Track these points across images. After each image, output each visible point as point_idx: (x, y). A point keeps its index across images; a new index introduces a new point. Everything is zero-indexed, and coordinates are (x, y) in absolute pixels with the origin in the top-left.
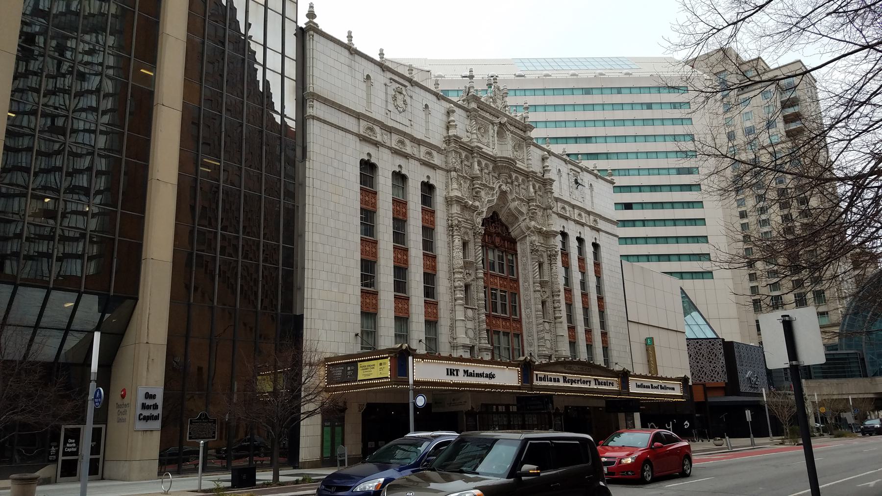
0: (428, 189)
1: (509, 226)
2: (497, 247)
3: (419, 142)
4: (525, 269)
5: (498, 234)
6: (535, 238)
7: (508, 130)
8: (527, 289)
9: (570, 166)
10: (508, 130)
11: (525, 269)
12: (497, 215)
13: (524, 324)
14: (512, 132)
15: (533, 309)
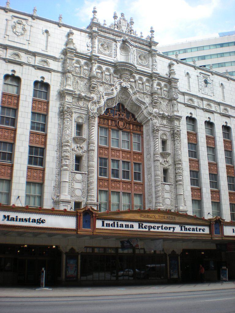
0: (42, 86)
1: (135, 114)
2: (121, 129)
3: (34, 54)
4: (148, 145)
5: (121, 119)
6: (157, 122)
7: (131, 45)
8: (149, 160)
9: (200, 71)
10: (131, 45)
11: (148, 145)
12: (123, 106)
13: (146, 186)
15: (153, 175)
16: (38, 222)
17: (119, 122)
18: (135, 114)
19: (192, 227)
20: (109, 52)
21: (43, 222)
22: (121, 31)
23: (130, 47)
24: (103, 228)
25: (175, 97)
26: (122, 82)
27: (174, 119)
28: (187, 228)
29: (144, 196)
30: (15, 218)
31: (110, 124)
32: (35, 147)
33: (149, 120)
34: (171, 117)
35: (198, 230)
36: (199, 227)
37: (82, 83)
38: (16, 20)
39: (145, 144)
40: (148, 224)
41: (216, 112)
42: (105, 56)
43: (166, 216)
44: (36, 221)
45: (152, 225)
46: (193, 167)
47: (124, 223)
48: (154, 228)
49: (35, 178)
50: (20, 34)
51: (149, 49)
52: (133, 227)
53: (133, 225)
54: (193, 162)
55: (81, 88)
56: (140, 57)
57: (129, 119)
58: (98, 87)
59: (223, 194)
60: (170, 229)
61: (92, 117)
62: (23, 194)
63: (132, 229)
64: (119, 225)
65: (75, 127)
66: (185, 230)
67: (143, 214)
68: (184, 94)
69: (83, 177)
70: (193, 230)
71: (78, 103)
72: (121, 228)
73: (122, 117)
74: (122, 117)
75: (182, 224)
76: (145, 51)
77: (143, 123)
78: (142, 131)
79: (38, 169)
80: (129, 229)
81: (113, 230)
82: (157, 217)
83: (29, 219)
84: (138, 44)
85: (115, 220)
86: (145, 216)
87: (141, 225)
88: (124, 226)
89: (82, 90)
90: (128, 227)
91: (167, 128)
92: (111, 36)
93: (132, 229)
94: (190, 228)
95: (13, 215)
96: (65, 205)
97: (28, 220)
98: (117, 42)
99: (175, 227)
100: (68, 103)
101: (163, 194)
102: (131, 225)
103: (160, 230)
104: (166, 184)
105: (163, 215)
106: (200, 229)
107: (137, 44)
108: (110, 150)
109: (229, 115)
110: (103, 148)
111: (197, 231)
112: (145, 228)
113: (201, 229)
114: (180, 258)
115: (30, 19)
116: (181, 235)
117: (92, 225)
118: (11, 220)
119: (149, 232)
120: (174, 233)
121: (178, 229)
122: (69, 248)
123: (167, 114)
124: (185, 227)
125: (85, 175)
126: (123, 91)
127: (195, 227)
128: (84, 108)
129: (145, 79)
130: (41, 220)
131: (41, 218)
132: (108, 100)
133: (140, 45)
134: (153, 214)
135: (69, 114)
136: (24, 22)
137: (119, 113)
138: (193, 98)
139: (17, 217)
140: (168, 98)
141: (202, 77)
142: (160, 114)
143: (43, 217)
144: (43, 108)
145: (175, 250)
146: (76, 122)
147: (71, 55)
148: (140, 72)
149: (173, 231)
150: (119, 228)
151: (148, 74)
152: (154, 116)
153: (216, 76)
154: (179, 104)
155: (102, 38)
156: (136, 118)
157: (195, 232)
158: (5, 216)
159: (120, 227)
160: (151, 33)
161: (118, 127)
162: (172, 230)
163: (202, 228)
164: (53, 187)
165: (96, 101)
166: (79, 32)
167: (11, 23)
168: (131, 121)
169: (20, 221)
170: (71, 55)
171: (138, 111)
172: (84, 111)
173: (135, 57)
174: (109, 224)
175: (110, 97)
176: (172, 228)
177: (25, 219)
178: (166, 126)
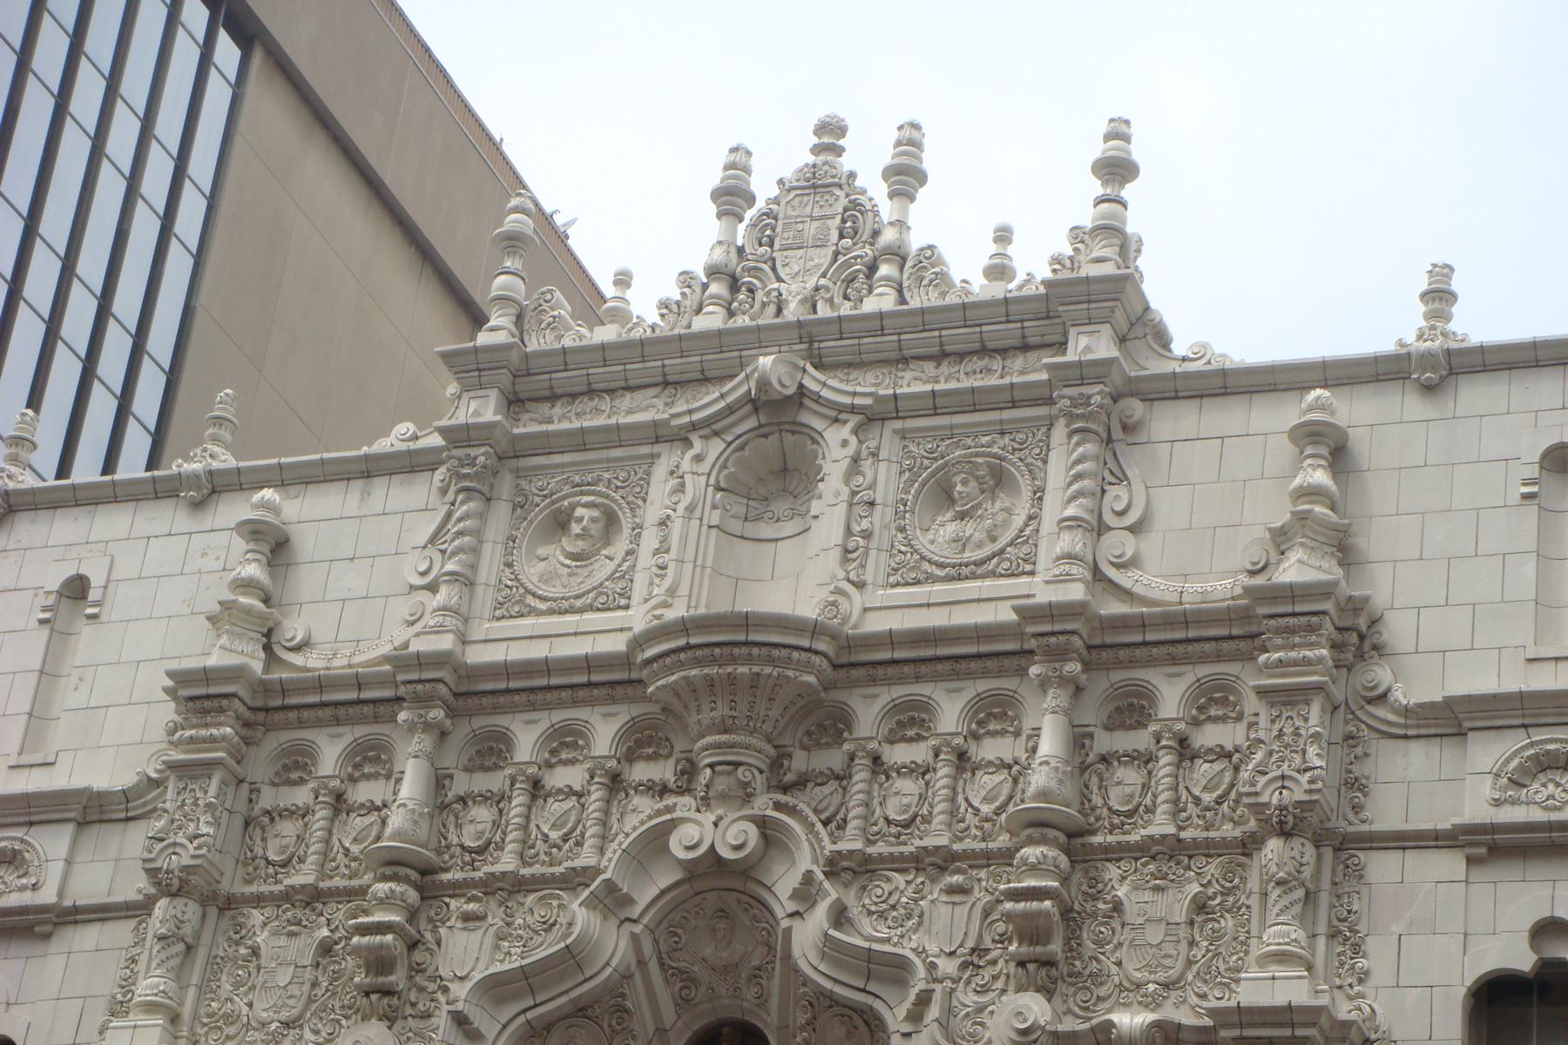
10: (838, 413)
14: (871, 417)
22: (768, 318)
25: (1264, 799)
26: (673, 824)
58: (439, 944)
76: (1008, 414)
84: (929, 367)
107: (912, 383)
147: (203, 732)
151: (983, 649)
155: (557, 459)
166: (357, 485)
170: (203, 732)
175: (554, 1003)
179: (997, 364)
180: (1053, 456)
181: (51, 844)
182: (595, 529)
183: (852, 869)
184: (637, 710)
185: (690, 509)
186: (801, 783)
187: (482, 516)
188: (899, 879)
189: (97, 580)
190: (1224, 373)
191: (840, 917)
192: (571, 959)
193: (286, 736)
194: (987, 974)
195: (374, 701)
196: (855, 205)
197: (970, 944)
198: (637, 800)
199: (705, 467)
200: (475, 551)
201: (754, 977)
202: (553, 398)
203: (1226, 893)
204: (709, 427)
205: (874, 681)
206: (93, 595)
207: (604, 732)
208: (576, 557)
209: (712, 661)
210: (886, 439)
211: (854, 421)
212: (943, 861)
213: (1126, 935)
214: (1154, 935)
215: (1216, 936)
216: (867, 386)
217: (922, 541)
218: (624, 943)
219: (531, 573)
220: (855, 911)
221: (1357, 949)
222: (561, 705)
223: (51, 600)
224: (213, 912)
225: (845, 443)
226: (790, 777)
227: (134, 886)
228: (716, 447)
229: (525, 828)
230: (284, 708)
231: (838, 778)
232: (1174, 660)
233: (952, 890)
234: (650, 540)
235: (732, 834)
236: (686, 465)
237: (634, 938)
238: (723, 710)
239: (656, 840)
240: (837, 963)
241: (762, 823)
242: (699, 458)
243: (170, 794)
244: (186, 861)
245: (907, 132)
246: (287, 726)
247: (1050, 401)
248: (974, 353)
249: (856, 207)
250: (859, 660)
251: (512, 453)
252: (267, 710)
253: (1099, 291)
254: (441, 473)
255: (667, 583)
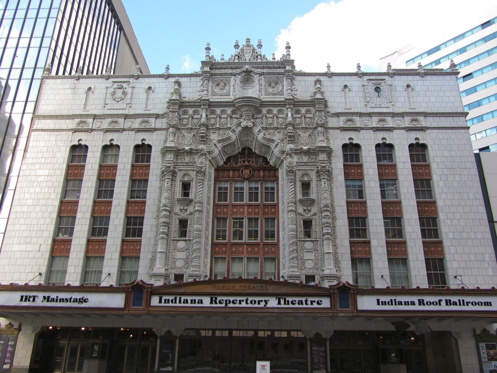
2: (246, 179)
5: (246, 167)
10: (256, 74)
12: (250, 149)
14: (261, 74)
16: (80, 302)
17: (243, 171)
18: (267, 157)
19: (297, 299)
20: (227, 91)
21: (85, 301)
22: (244, 61)
23: (256, 76)
24: (160, 305)
26: (241, 122)
27: (319, 152)
28: (288, 301)
29: (279, 260)
30: (55, 298)
31: (231, 175)
32: (134, 217)
33: (282, 161)
34: (314, 150)
35: (309, 302)
36: (310, 299)
37: (189, 135)
38: (116, 85)
39: (280, 192)
40: (225, 298)
41: (396, 128)
42: (222, 97)
43: (252, 285)
44: (78, 301)
45: (232, 299)
46: (357, 212)
47: (189, 298)
48: (233, 302)
49: (131, 251)
50: (119, 100)
51: (282, 71)
52: (202, 303)
53: (202, 301)
54: (356, 204)
55: (187, 142)
56: (270, 85)
57: (258, 164)
58: (210, 135)
59: (412, 245)
60: (259, 303)
61: (198, 171)
62: (114, 271)
63: (200, 305)
64: (182, 301)
65: (180, 187)
66: (285, 304)
67: (216, 285)
68: (338, 115)
69: (186, 244)
70: (301, 303)
71: (183, 160)
72: (186, 305)
73: (246, 164)
74: (246, 164)
75: (279, 295)
77: (277, 167)
78: (277, 176)
79: (135, 242)
80: (197, 305)
81: (175, 307)
82: (238, 287)
83: (71, 299)
84: (267, 69)
85: (176, 294)
86: (219, 287)
87: (214, 299)
88: (189, 301)
89: (189, 143)
90: (195, 303)
91: (309, 165)
92: (230, 71)
93: (200, 305)
94: (295, 301)
95: (53, 295)
96: (157, 279)
97: (69, 300)
98: (237, 75)
99: (268, 300)
100: (168, 162)
101: (302, 255)
102: (199, 300)
103: (244, 304)
104: (306, 241)
105: (248, 285)
106: (312, 302)
107: (265, 71)
108: (230, 207)
109: (422, 127)
110: (221, 206)
111: (306, 304)
112: (220, 302)
113: (314, 301)
114: (330, 343)
115: (131, 80)
116: (276, 311)
117: (144, 302)
118: (51, 301)
119: (226, 308)
120: (266, 308)
121: (273, 303)
122: (165, 330)
123: (305, 148)
124: (285, 299)
125: (189, 241)
126: (246, 132)
127: (303, 299)
128: (190, 163)
129: (275, 110)
130: (84, 299)
131: (83, 297)
132: (224, 147)
133: (269, 71)
134: (231, 285)
135: (169, 174)
136: (125, 85)
137: (244, 160)
138: (354, 118)
139: (57, 297)
140: (313, 126)
141: (372, 84)
142: (297, 150)
143: (86, 296)
144: (144, 173)
145: (321, 332)
146: (181, 181)
147: (174, 107)
148: (268, 104)
149: (265, 305)
150: (182, 305)
151: (279, 103)
152: (287, 154)
153: (397, 78)
154: (331, 131)
155: (217, 77)
156: (269, 162)
157: (304, 306)
158: (44, 297)
159: (184, 303)
160: (286, 50)
161: (242, 177)
162: (262, 304)
163: (316, 299)
164: (149, 260)
165: (206, 152)
166: (189, 78)
167: (111, 90)
168: (261, 166)
169: (60, 301)
170: (174, 107)
171: (268, 151)
172: (191, 167)
173: (263, 87)
174: (169, 300)
175: (227, 143)
176: (264, 301)
177: (66, 299)
178: (308, 164)
179: (276, 70)
180: (284, 81)
181: (152, 120)
182: (224, 86)
183: (266, 129)
184: (233, 108)
185: (237, 84)
186: (256, 118)
187: (208, 83)
188: (271, 131)
189: (153, 87)
190: (305, 73)
191: (264, 134)
192: (229, 138)
193: (184, 109)
194: (284, 142)
195: (197, 105)
196: (254, 49)
197: (282, 138)
198: (234, 119)
199: (239, 79)
200: (208, 87)
201: (251, 142)
202: (216, 69)
203: (313, 134)
204: (239, 74)
205: (265, 107)
206: (153, 89)
207: (229, 111)
208: (222, 89)
209: (246, 102)
210: (262, 77)
211: (258, 75)
212: (277, 128)
213: (301, 138)
214: (305, 138)
215: (312, 139)
216: (259, 71)
217: (268, 90)
218: (235, 136)
219: (216, 91)
220: (266, 134)
221: (329, 140)
222: (222, 107)
223: (147, 89)
224: (177, 130)
225: (257, 78)
226: (255, 118)
227: (165, 126)
228: (240, 77)
229: (219, 122)
230: (184, 105)
231: (261, 118)
232: (303, 106)
233: (278, 132)
234: (232, 88)
235: (250, 124)
236: (236, 78)
237: (236, 136)
238: (247, 109)
239: (239, 124)
240: (264, 140)
241: (253, 123)
242: (238, 78)
243: (170, 115)
244: (174, 123)
245: (260, 41)
246: (184, 107)
247: (283, 75)
248: (272, 68)
249: (254, 49)
250: (263, 104)
251: (212, 75)
252: (181, 105)
253: (287, 62)
254: (201, 77)
255: (235, 93)
